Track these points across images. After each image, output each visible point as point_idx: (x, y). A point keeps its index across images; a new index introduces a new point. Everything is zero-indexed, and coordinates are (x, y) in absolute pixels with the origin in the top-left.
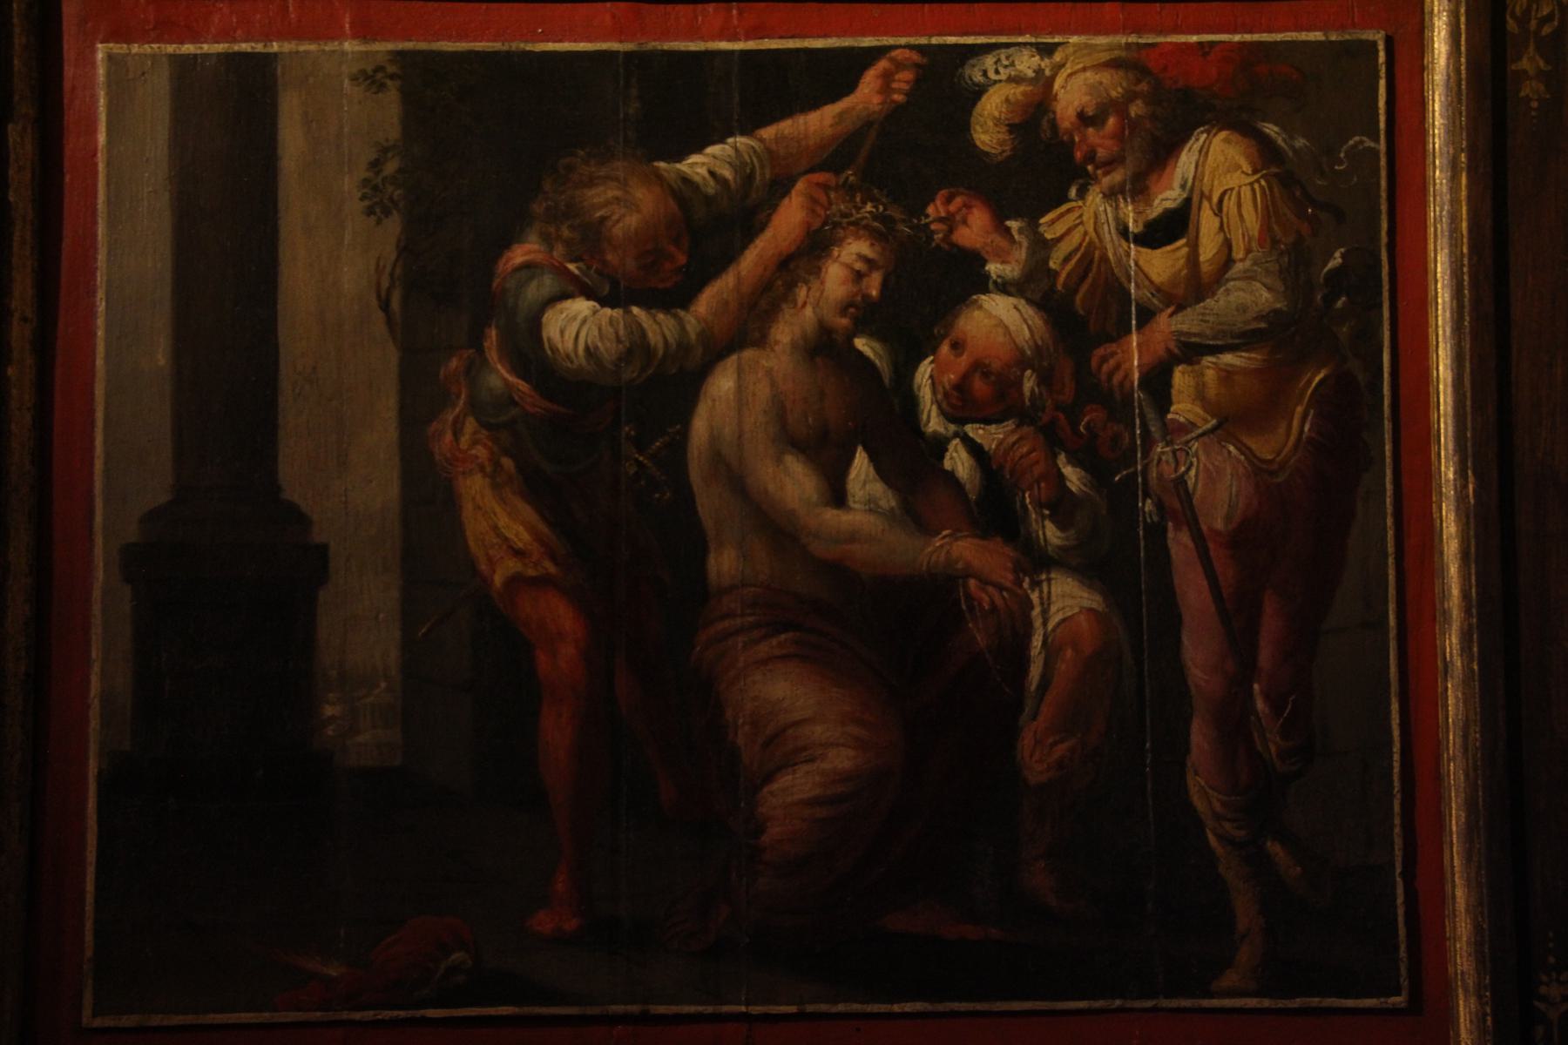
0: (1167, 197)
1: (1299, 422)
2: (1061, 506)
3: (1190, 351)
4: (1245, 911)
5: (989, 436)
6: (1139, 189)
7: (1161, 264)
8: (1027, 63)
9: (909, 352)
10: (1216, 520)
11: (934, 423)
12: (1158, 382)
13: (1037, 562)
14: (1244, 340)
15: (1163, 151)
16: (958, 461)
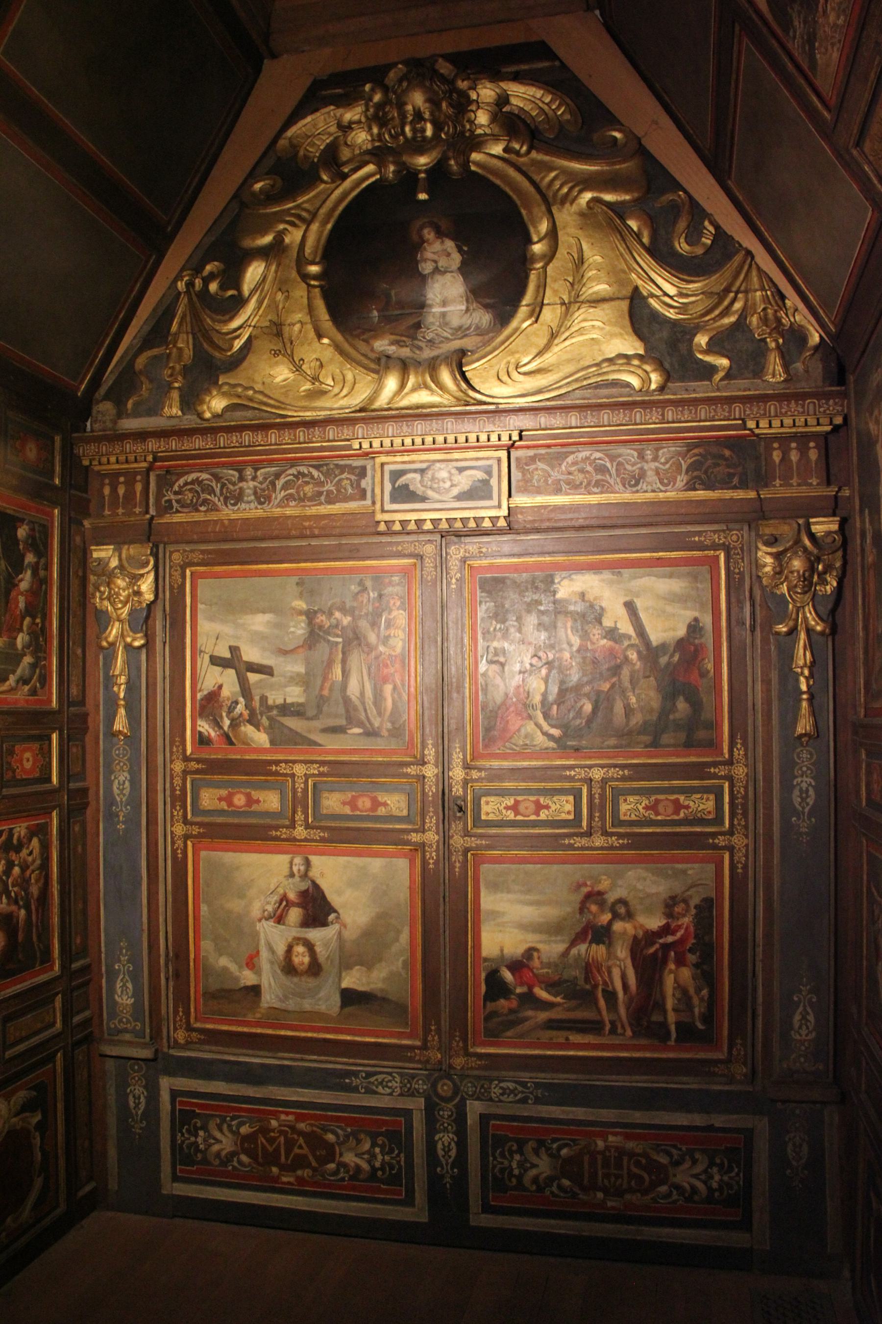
0: (31, 848)
1: (42, 881)
2: (22, 898)
3: (33, 871)
4: (38, 954)
5: (16, 889)
6: (28, 848)
7: (30, 859)
8: (18, 829)
9: (8, 878)
10: (35, 896)
11: (10, 888)
12: (30, 877)
13: (19, 908)
14: (38, 869)
15: (30, 841)
16: (13, 894)
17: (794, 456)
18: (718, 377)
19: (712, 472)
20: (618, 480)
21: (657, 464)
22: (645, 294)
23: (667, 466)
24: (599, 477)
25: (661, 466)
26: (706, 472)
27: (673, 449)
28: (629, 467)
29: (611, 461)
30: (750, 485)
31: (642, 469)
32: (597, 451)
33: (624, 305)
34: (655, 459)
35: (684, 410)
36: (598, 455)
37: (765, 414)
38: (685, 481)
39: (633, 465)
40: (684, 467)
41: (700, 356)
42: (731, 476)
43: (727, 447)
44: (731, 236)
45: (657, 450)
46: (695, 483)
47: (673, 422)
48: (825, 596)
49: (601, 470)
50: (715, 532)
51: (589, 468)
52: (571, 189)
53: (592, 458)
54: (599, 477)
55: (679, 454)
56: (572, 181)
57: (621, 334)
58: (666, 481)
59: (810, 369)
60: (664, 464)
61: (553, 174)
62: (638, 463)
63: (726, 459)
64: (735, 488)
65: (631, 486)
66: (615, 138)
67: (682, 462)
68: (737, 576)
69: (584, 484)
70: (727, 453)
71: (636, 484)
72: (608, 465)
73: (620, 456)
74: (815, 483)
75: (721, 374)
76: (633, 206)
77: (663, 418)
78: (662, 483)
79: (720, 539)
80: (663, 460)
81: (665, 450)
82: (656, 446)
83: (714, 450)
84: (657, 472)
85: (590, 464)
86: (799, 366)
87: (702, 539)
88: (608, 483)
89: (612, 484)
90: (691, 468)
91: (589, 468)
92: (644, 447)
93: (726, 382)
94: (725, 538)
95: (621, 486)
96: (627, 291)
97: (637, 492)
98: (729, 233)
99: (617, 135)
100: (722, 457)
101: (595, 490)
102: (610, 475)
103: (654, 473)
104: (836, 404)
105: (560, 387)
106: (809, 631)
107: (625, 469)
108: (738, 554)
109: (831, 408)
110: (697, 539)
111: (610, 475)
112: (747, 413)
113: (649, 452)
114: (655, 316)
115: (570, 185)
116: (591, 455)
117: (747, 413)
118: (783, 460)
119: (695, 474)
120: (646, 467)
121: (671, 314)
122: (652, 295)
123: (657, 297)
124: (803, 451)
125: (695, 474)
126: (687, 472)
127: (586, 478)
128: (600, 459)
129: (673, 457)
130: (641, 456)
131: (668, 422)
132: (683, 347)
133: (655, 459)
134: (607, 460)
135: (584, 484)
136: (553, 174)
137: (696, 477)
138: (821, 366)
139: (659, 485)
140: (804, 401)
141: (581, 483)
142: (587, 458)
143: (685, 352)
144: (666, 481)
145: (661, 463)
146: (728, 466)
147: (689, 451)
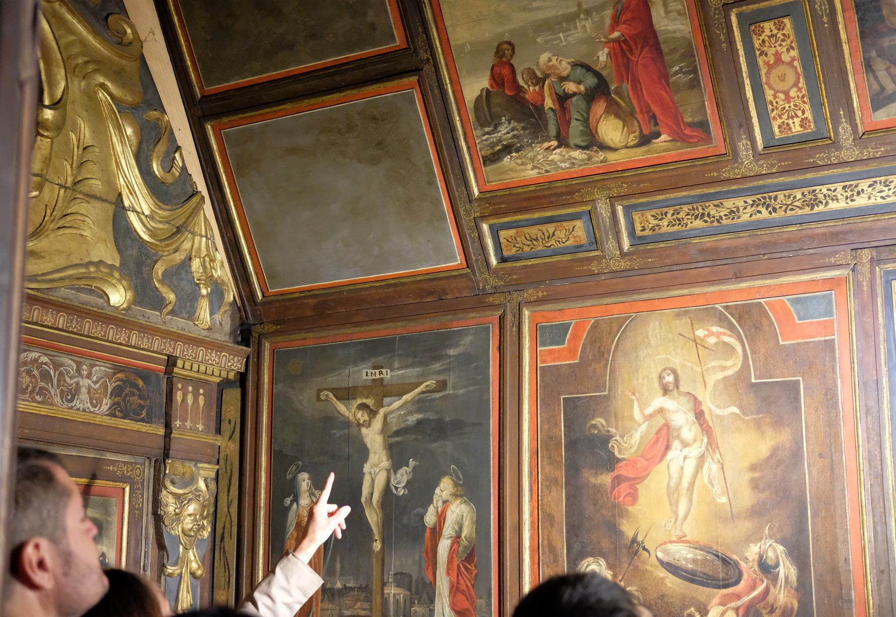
17: (190, 399)
18: (165, 311)
19: (129, 400)
20: (58, 391)
21: (90, 382)
22: (127, 203)
23: (98, 386)
24: (43, 384)
25: (92, 385)
26: (124, 400)
27: (103, 368)
28: (68, 379)
29: (55, 370)
30: (154, 420)
31: (77, 384)
32: (45, 354)
33: (111, 209)
34: (89, 376)
35: (144, 336)
36: (45, 359)
37: (195, 358)
38: (108, 405)
39: (71, 378)
40: (110, 390)
41: (157, 285)
42: (142, 407)
43: (141, 378)
44: (190, 175)
45: (92, 366)
46: (115, 409)
47: (134, 347)
48: (202, 540)
49: (45, 376)
50: (124, 463)
51: (36, 372)
52: (86, 63)
53: (40, 361)
54: (43, 384)
55: (107, 375)
56: (85, 55)
57: (105, 241)
58: (94, 402)
59: (223, 323)
60: (95, 383)
61: (72, 38)
62: (75, 377)
63: (139, 390)
64: (143, 420)
65: (68, 401)
66: (126, 32)
67: (109, 384)
68: (137, 512)
69: (30, 389)
70: (141, 383)
71: (71, 400)
72: (52, 372)
73: (62, 365)
74: (200, 429)
75: (170, 308)
76: (128, 109)
77: (128, 342)
78: (91, 403)
79: (128, 472)
80: (94, 379)
81: (97, 368)
82: (92, 362)
83: (132, 377)
84: (89, 388)
85: (38, 369)
86: (217, 317)
87: (116, 469)
88: (50, 393)
89: (53, 394)
90: (117, 392)
91: (36, 372)
92: (82, 360)
93: (170, 317)
94: (132, 471)
95: (59, 399)
96: (113, 197)
97: (71, 408)
98: (190, 173)
99: (129, 31)
100: (135, 386)
101: (38, 398)
102: (52, 385)
103: (87, 391)
104: (238, 361)
105: (53, 281)
106: (193, 574)
107: (65, 381)
108: (139, 489)
109: (144, 344)
110: (111, 468)
111: (52, 385)
112: (185, 353)
113: (85, 367)
114: (130, 230)
115: (86, 59)
116: (39, 357)
117: (185, 353)
118: (183, 401)
119: (117, 399)
120: (81, 384)
121: (146, 237)
122: (134, 211)
123: (137, 212)
124: (196, 396)
125: (117, 399)
126: (111, 395)
127: (32, 383)
128: (46, 364)
129: (102, 378)
130: (79, 371)
131: (153, 352)
132: (145, 269)
133: (89, 376)
134: (51, 367)
135: (30, 389)
136: (72, 38)
137: (117, 403)
138: (230, 323)
139: (89, 405)
140: (221, 352)
141: (27, 387)
142: (36, 360)
143: (146, 278)
144: (94, 402)
145: (93, 382)
146: (141, 397)
147: (115, 374)
